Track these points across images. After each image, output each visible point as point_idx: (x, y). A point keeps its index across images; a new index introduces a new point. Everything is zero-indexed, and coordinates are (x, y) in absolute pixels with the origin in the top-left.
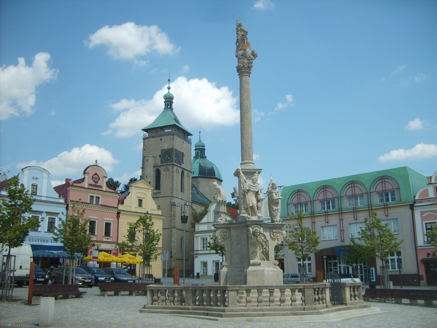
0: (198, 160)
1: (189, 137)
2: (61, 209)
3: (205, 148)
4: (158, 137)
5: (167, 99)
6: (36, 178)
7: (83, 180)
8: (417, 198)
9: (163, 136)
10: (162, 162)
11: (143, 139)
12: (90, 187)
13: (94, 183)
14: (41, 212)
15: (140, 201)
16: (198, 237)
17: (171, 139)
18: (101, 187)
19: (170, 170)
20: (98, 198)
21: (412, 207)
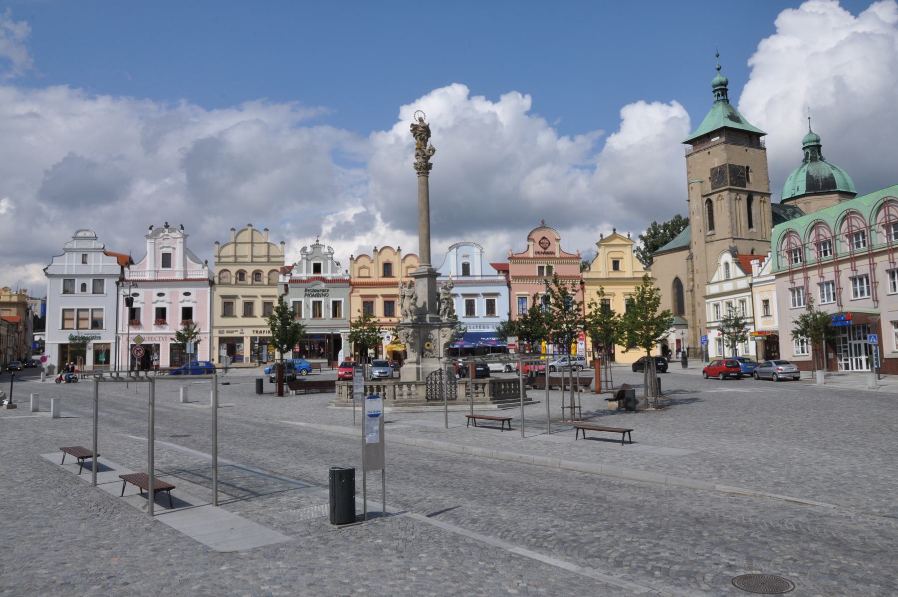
0: (806, 167)
1: (762, 138)
2: (504, 290)
3: (821, 143)
5: (716, 86)
6: (467, 256)
10: (713, 188)
11: (687, 156)
12: (538, 256)
13: (543, 250)
14: (476, 295)
15: (616, 265)
16: (709, 303)
18: (552, 253)
20: (550, 268)
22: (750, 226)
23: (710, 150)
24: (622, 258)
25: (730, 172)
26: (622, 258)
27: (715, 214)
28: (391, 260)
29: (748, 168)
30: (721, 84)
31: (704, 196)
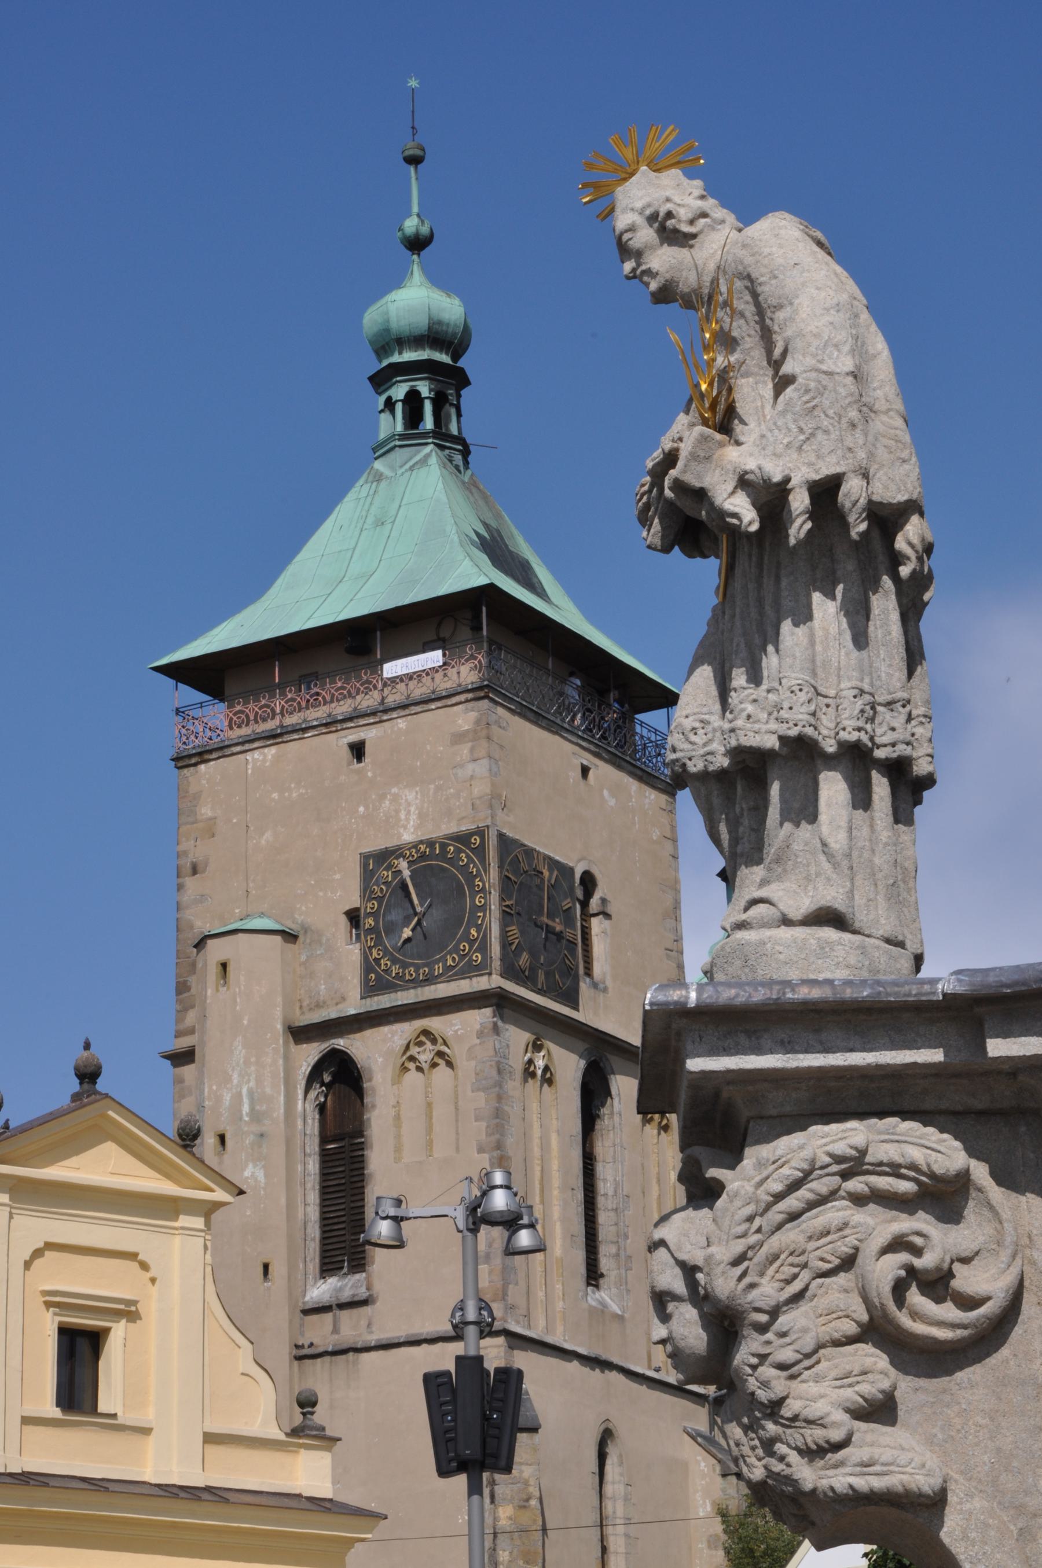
1: (653, 718)
4: (330, 724)
5: (402, 342)
9: (382, 712)
10: (374, 985)
15: (80, 1351)
17: (458, 738)
19: (456, 1052)
22: (593, 1276)
23: (370, 734)
24: (129, 1312)
25: (506, 883)
26: (129, 1312)
29: (589, 881)
30: (433, 336)
31: (300, 1034)
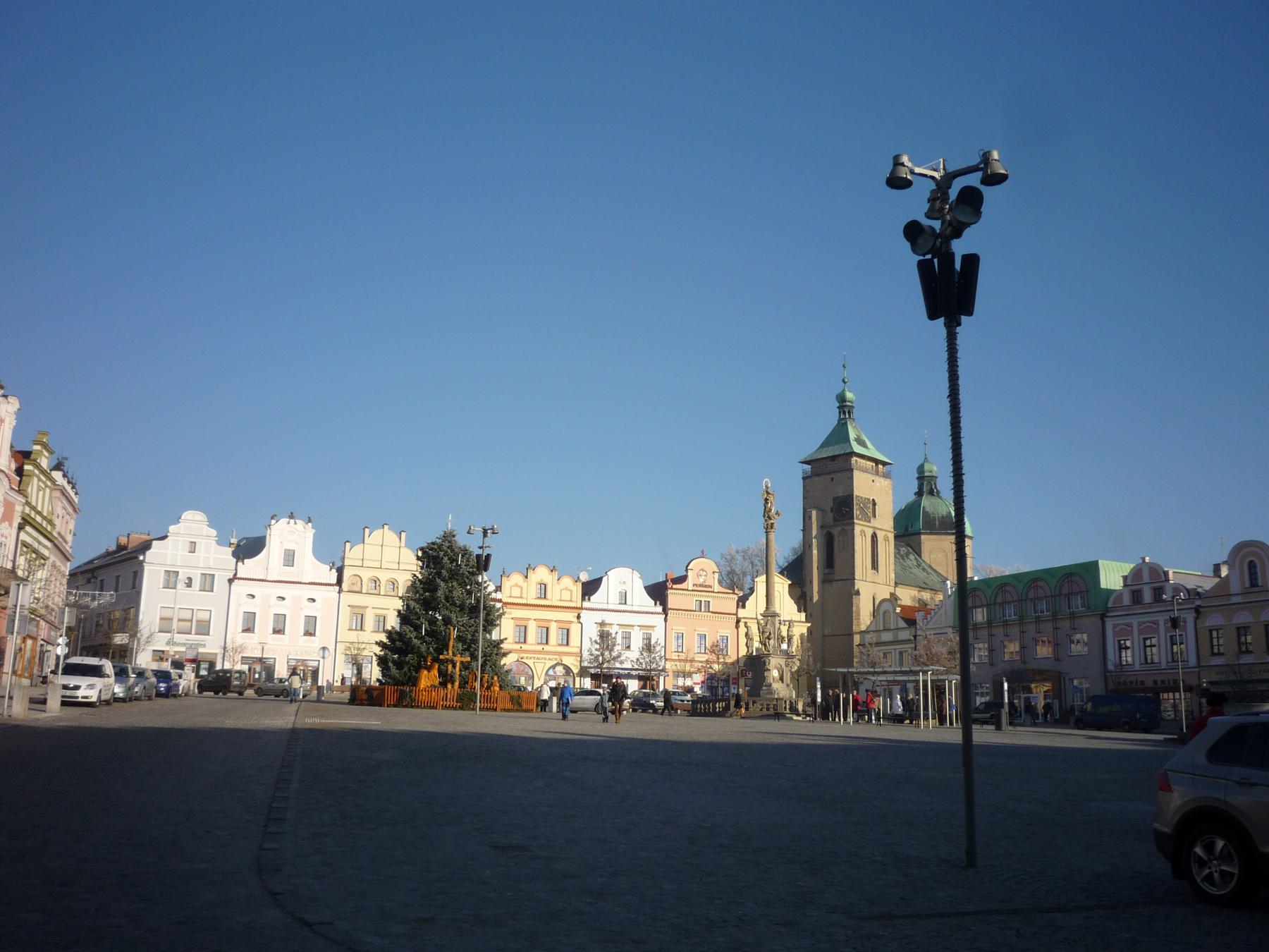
7: (682, 579)
8: (1110, 605)
10: (835, 520)
21: (1103, 617)
27: (836, 550)
28: (545, 581)
